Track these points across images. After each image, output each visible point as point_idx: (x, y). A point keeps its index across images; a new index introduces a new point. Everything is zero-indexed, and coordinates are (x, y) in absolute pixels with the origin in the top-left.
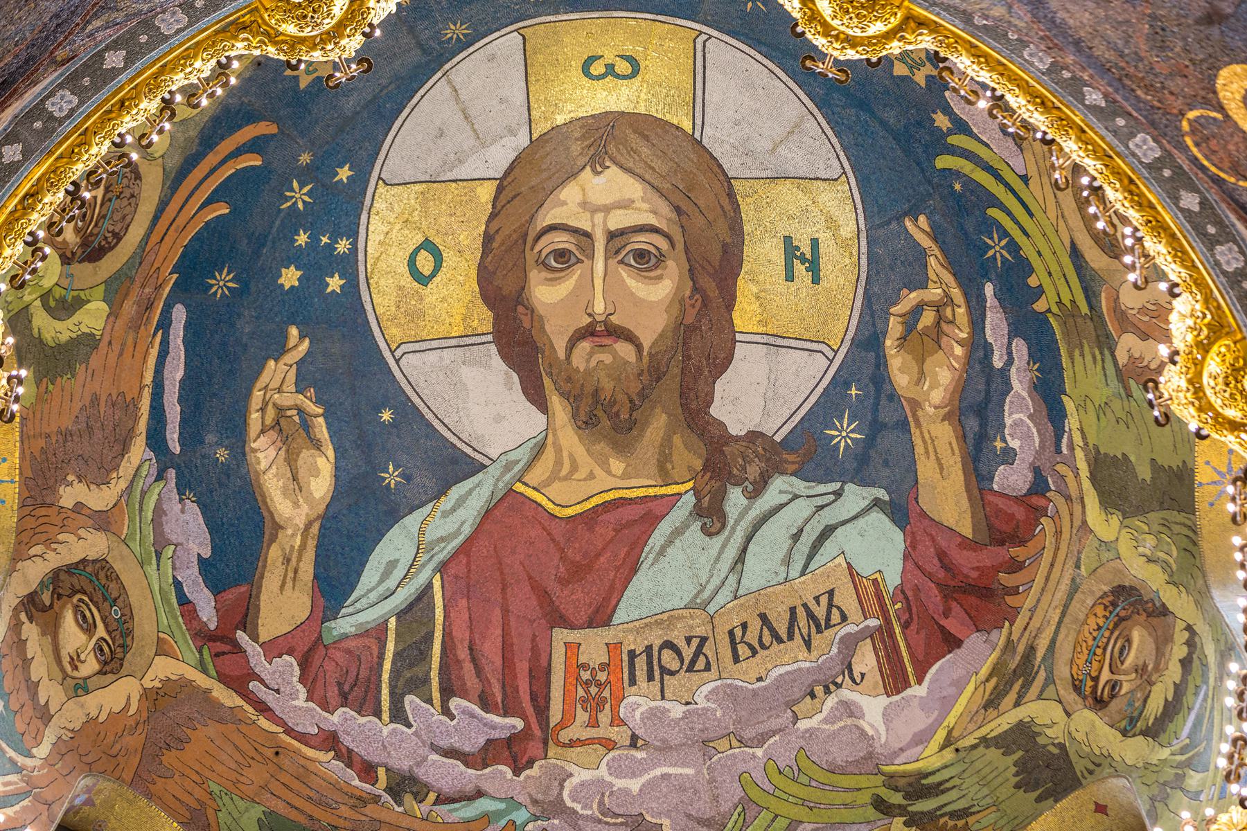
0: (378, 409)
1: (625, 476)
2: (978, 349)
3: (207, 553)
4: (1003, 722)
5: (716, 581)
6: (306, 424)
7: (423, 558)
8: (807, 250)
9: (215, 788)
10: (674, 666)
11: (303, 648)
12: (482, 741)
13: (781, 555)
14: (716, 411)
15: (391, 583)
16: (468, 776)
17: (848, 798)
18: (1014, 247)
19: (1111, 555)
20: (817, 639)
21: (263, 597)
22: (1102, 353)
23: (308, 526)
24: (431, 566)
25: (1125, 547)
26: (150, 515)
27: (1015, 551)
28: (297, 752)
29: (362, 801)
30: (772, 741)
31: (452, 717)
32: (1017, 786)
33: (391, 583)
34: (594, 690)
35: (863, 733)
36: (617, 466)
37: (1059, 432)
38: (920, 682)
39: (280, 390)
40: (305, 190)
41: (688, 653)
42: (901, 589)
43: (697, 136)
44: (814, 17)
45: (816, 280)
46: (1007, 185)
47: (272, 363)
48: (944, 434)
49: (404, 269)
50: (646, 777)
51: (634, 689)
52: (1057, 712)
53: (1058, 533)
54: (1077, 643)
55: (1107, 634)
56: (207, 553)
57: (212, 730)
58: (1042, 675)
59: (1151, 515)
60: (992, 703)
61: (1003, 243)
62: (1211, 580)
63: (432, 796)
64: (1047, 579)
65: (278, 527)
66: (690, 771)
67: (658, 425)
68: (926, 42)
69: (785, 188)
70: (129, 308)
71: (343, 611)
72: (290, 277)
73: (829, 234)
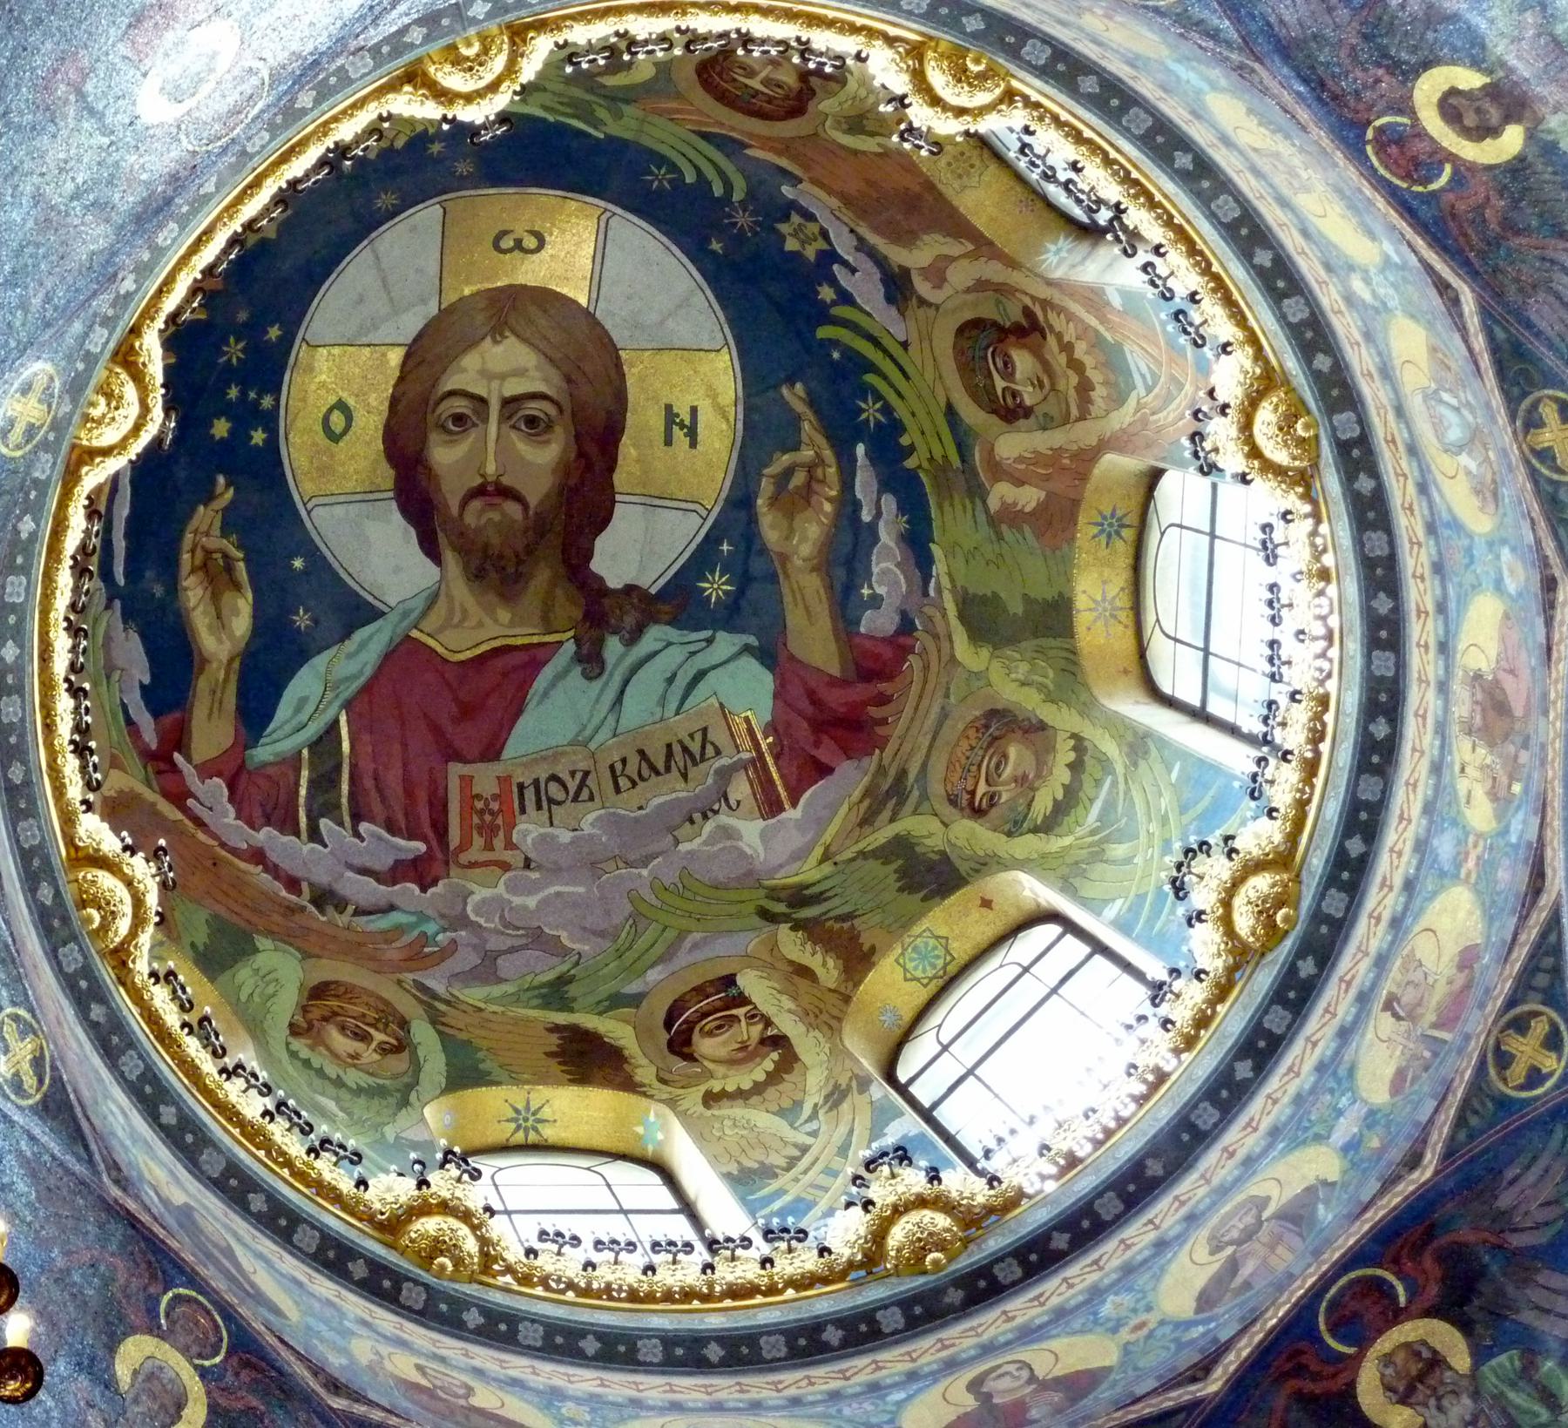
0: (291, 557)
2: (848, 505)
4: (882, 834)
5: (596, 721)
6: (229, 568)
7: (330, 695)
10: (560, 796)
11: (231, 768)
12: (390, 862)
13: (655, 697)
14: (597, 565)
17: (733, 909)
18: (887, 410)
19: (981, 683)
20: (693, 772)
21: (194, 723)
22: (973, 502)
23: (231, 661)
24: (337, 704)
25: (996, 673)
26: (100, 640)
27: (883, 686)
28: (231, 864)
29: (292, 910)
30: (655, 862)
31: (363, 840)
32: (901, 890)
33: (304, 717)
34: (488, 818)
35: (742, 854)
36: (504, 615)
37: (926, 578)
38: (794, 804)
40: (240, 346)
41: (573, 785)
42: (771, 728)
45: (693, 444)
46: (885, 351)
47: (201, 508)
48: (812, 584)
49: (319, 428)
50: (541, 895)
51: (524, 817)
52: (934, 825)
53: (926, 668)
54: (950, 762)
55: (981, 753)
56: (147, 680)
58: (916, 793)
59: (1024, 644)
60: (867, 821)
61: (878, 406)
62: (1096, 692)
63: (351, 909)
64: (916, 709)
65: (205, 661)
66: (581, 890)
67: (542, 577)
69: (666, 357)
71: (262, 741)
72: (221, 428)
73: (708, 402)
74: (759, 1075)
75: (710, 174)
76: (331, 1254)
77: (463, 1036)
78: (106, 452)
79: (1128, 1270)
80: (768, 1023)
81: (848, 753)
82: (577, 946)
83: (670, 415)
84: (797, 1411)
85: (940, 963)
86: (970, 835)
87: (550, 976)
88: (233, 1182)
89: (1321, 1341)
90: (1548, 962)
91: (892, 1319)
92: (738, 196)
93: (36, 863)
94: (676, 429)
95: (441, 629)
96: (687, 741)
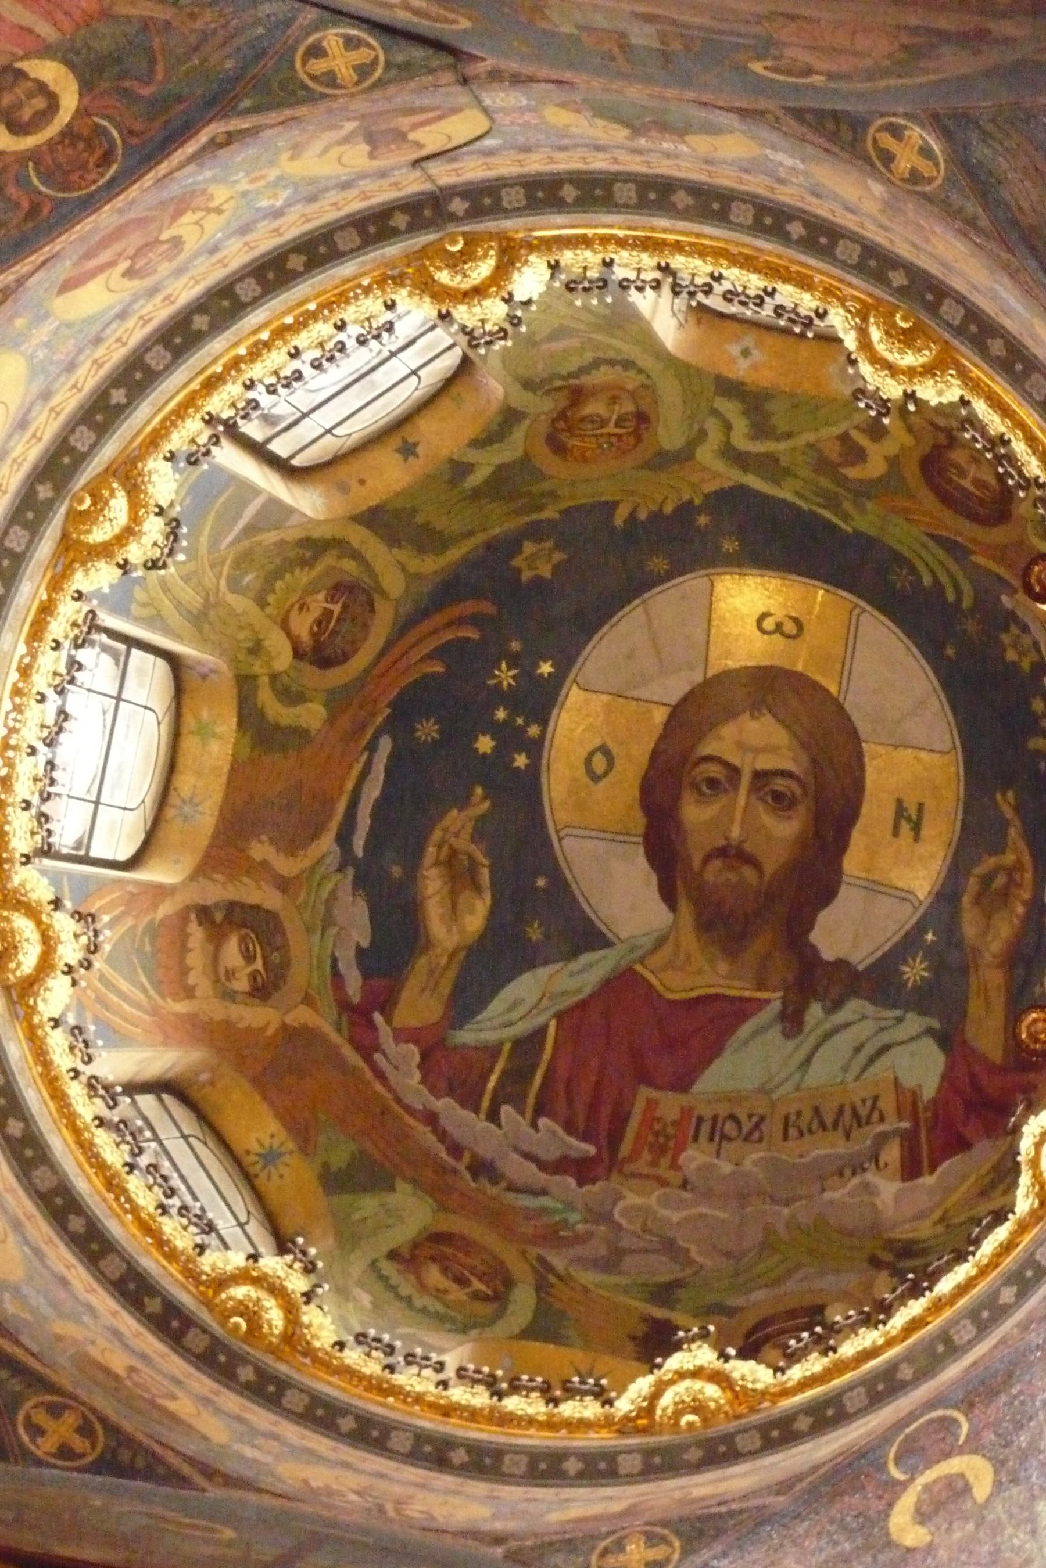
1: (729, 977)
3: (365, 944)
6: (473, 867)
7: (545, 1001)
8: (913, 813)
9: (323, 1117)
10: (734, 1133)
14: (816, 937)
15: (514, 1015)
16: (542, 1178)
24: (552, 1011)
27: (1031, 1076)
29: (442, 1169)
33: (514, 1015)
34: (662, 1140)
36: (723, 967)
39: (457, 835)
40: (511, 674)
41: (747, 1126)
42: (934, 1101)
43: (841, 699)
44: (865, 343)
45: (916, 839)
50: (685, 1213)
51: (694, 1145)
56: (365, 944)
63: (503, 1184)
65: (428, 945)
66: (722, 1215)
70: (345, 722)
71: (467, 1026)
72: (485, 744)
75: (944, 579)
77: (558, 1305)
82: (699, 1259)
92: (967, 603)
94: (903, 822)
96: (859, 1104)
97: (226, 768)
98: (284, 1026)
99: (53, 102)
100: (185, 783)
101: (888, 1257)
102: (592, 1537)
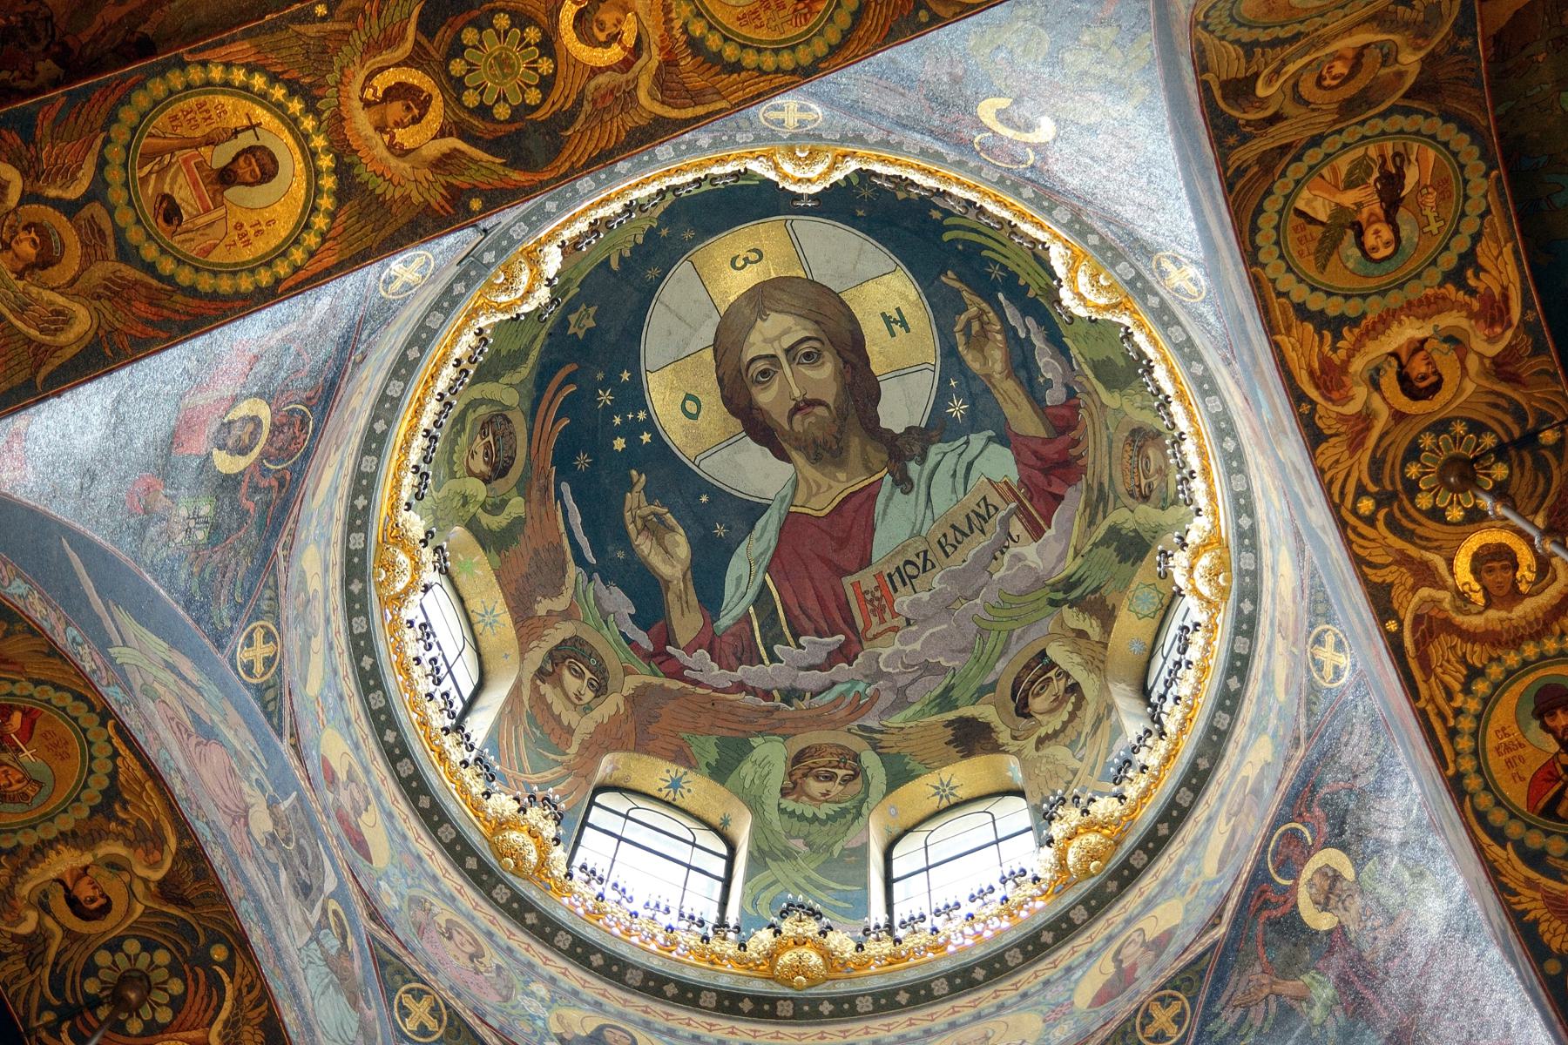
2: (1009, 332)
3: (633, 611)
4: (1100, 531)
5: (920, 518)
6: (660, 518)
9: (684, 735)
10: (915, 572)
12: (825, 655)
14: (883, 424)
15: (743, 588)
17: (1034, 606)
18: (1004, 268)
20: (986, 527)
23: (684, 576)
25: (1128, 408)
27: (1072, 434)
33: (743, 588)
36: (842, 476)
41: (920, 562)
42: (1021, 481)
45: (908, 330)
48: (1010, 386)
52: (1125, 513)
53: (1091, 415)
56: (633, 611)
57: (672, 705)
60: (1091, 523)
65: (667, 582)
67: (855, 444)
68: (852, 166)
70: (535, 494)
72: (619, 444)
74: (1065, 717)
76: (727, 1003)
77: (894, 751)
78: (406, 591)
79: (1195, 843)
80: (1068, 676)
81: (1069, 483)
83: (887, 319)
84: (1023, 1004)
85: (1157, 600)
86: (1144, 515)
87: (939, 690)
88: (651, 984)
89: (1273, 880)
90: (1320, 596)
91: (1079, 915)
93: (458, 848)
95: (808, 500)
97: (494, 579)
98: (626, 698)
99: (256, 421)
100: (474, 605)
101: (1060, 596)
102: (1128, 1020)
